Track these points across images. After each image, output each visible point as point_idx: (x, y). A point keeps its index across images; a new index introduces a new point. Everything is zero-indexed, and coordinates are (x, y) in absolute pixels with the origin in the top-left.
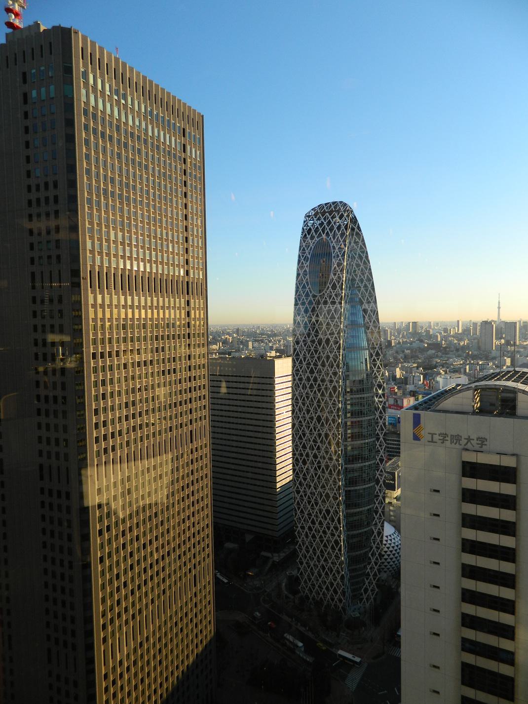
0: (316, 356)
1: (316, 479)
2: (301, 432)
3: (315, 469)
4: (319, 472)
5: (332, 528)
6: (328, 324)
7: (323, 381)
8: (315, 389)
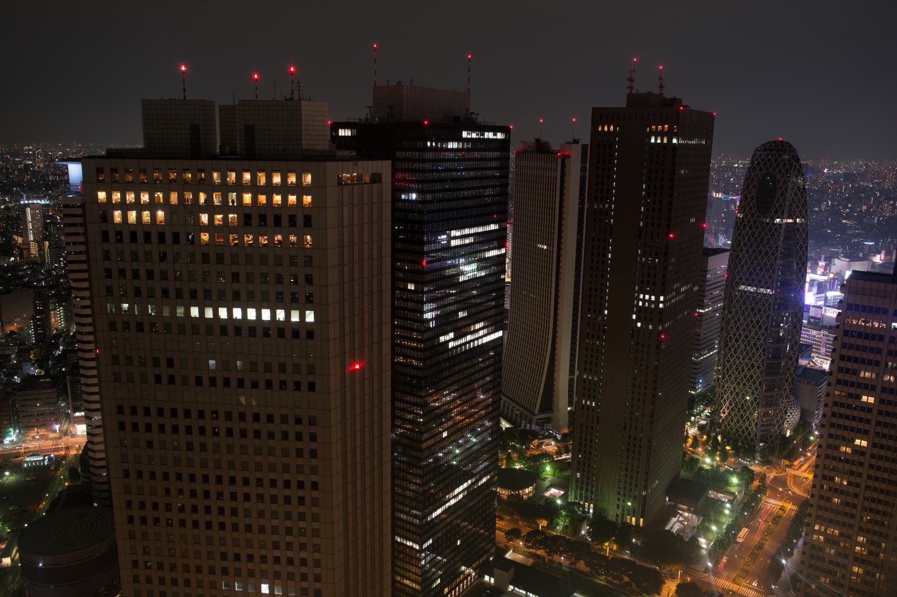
0: (756, 263)
1: (745, 353)
2: (736, 318)
3: (745, 346)
4: (748, 348)
6: (769, 240)
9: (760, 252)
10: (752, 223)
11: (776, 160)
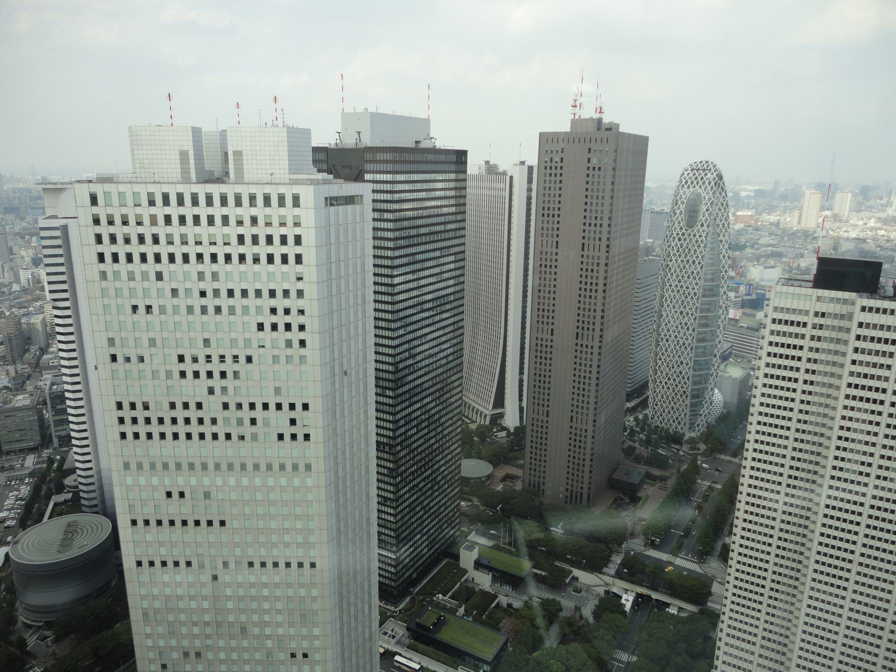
0: (684, 271)
1: (674, 351)
2: (667, 320)
5: (682, 382)
6: (695, 251)
7: (687, 288)
8: (681, 292)
9: (688, 261)
10: (680, 235)
11: (702, 178)
